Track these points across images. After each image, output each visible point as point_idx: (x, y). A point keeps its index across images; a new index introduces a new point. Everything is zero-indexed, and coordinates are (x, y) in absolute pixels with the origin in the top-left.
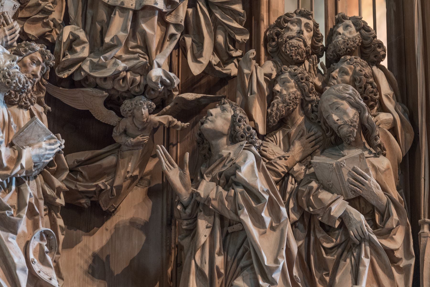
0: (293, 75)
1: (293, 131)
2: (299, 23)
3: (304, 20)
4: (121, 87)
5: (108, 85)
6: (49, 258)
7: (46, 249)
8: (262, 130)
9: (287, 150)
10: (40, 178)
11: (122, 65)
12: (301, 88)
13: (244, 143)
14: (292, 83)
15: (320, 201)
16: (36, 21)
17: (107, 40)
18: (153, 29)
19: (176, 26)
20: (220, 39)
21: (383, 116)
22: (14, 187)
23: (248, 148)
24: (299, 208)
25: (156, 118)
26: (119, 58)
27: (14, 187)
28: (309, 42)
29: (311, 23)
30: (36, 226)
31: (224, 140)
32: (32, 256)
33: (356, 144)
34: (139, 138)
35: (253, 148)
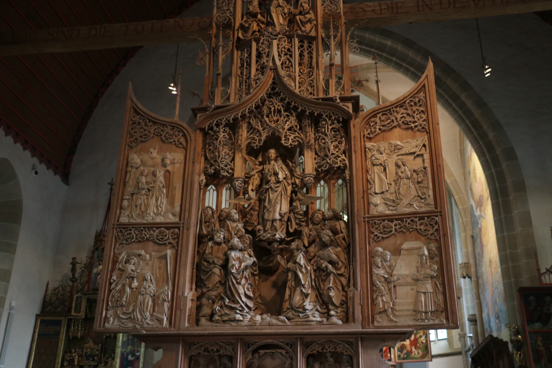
0: (314, 229)
1: (316, 243)
2: (317, 213)
3: (319, 212)
4: (270, 240)
5: (267, 240)
6: (250, 289)
7: (249, 287)
8: (307, 245)
9: (315, 249)
10: (250, 268)
11: (269, 235)
12: (317, 232)
13: (300, 251)
14: (314, 231)
15: (321, 263)
16: (251, 226)
17: (266, 229)
18: (277, 224)
19: (284, 221)
20: (297, 221)
21: (341, 235)
22: (241, 273)
23: (300, 252)
24: (316, 265)
25: (280, 247)
26: (269, 233)
27: (241, 273)
28: (321, 218)
29: (321, 212)
30: (247, 281)
31: (295, 251)
32: (245, 289)
33: (331, 245)
34: (277, 252)
35: (302, 252)
